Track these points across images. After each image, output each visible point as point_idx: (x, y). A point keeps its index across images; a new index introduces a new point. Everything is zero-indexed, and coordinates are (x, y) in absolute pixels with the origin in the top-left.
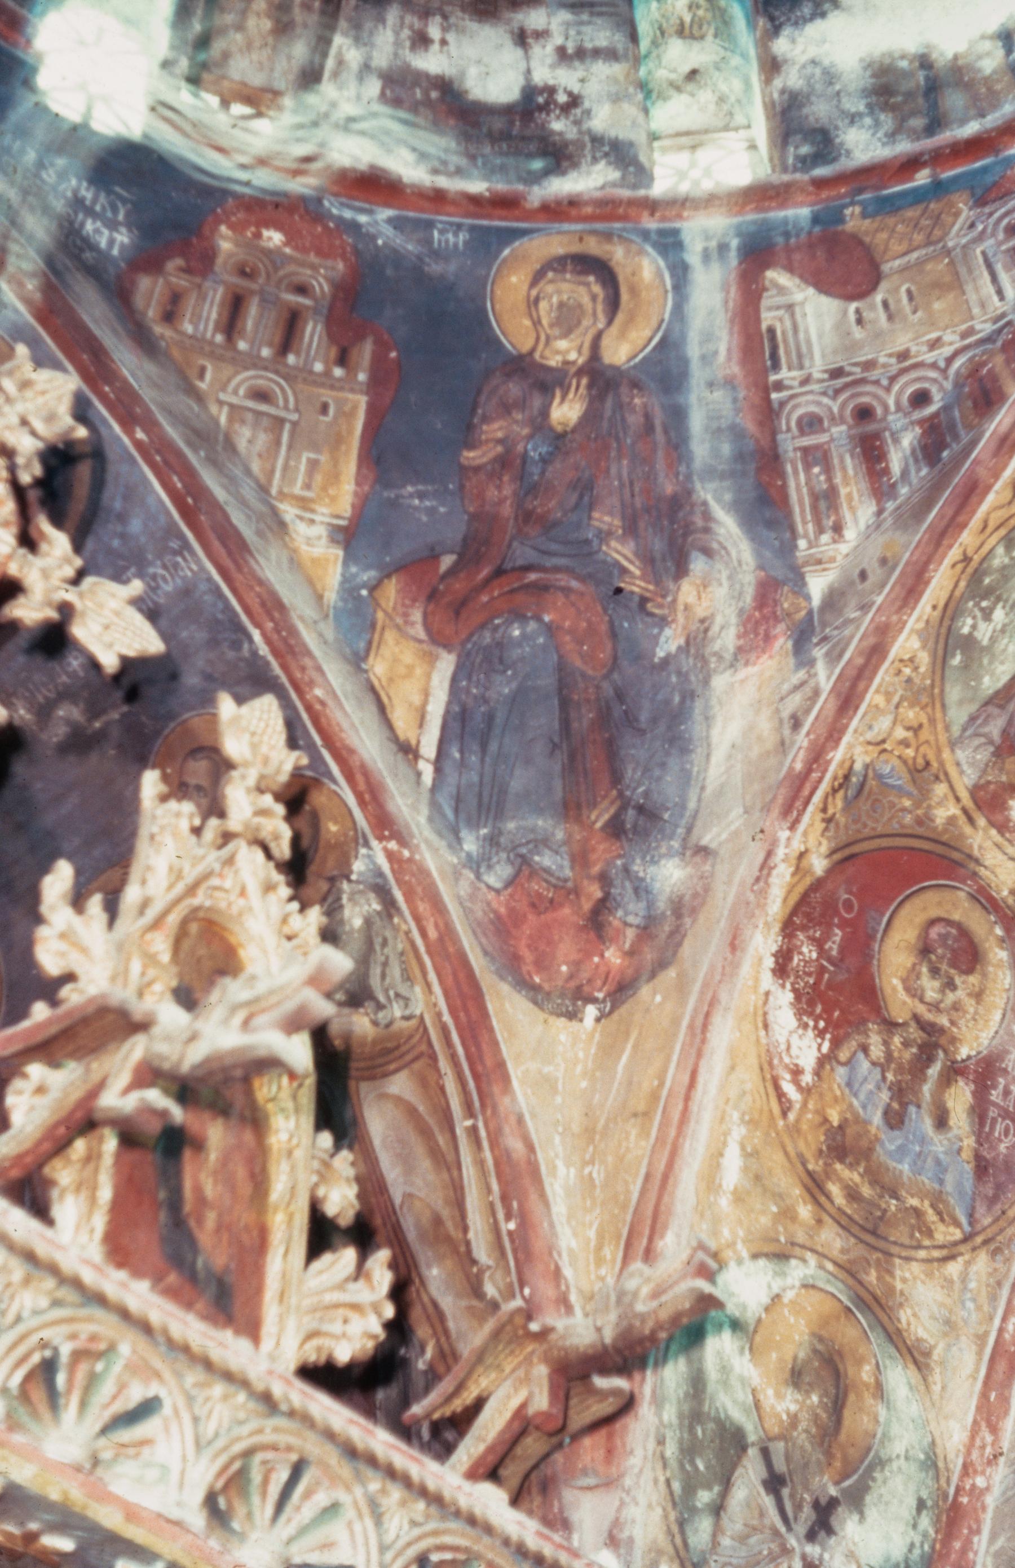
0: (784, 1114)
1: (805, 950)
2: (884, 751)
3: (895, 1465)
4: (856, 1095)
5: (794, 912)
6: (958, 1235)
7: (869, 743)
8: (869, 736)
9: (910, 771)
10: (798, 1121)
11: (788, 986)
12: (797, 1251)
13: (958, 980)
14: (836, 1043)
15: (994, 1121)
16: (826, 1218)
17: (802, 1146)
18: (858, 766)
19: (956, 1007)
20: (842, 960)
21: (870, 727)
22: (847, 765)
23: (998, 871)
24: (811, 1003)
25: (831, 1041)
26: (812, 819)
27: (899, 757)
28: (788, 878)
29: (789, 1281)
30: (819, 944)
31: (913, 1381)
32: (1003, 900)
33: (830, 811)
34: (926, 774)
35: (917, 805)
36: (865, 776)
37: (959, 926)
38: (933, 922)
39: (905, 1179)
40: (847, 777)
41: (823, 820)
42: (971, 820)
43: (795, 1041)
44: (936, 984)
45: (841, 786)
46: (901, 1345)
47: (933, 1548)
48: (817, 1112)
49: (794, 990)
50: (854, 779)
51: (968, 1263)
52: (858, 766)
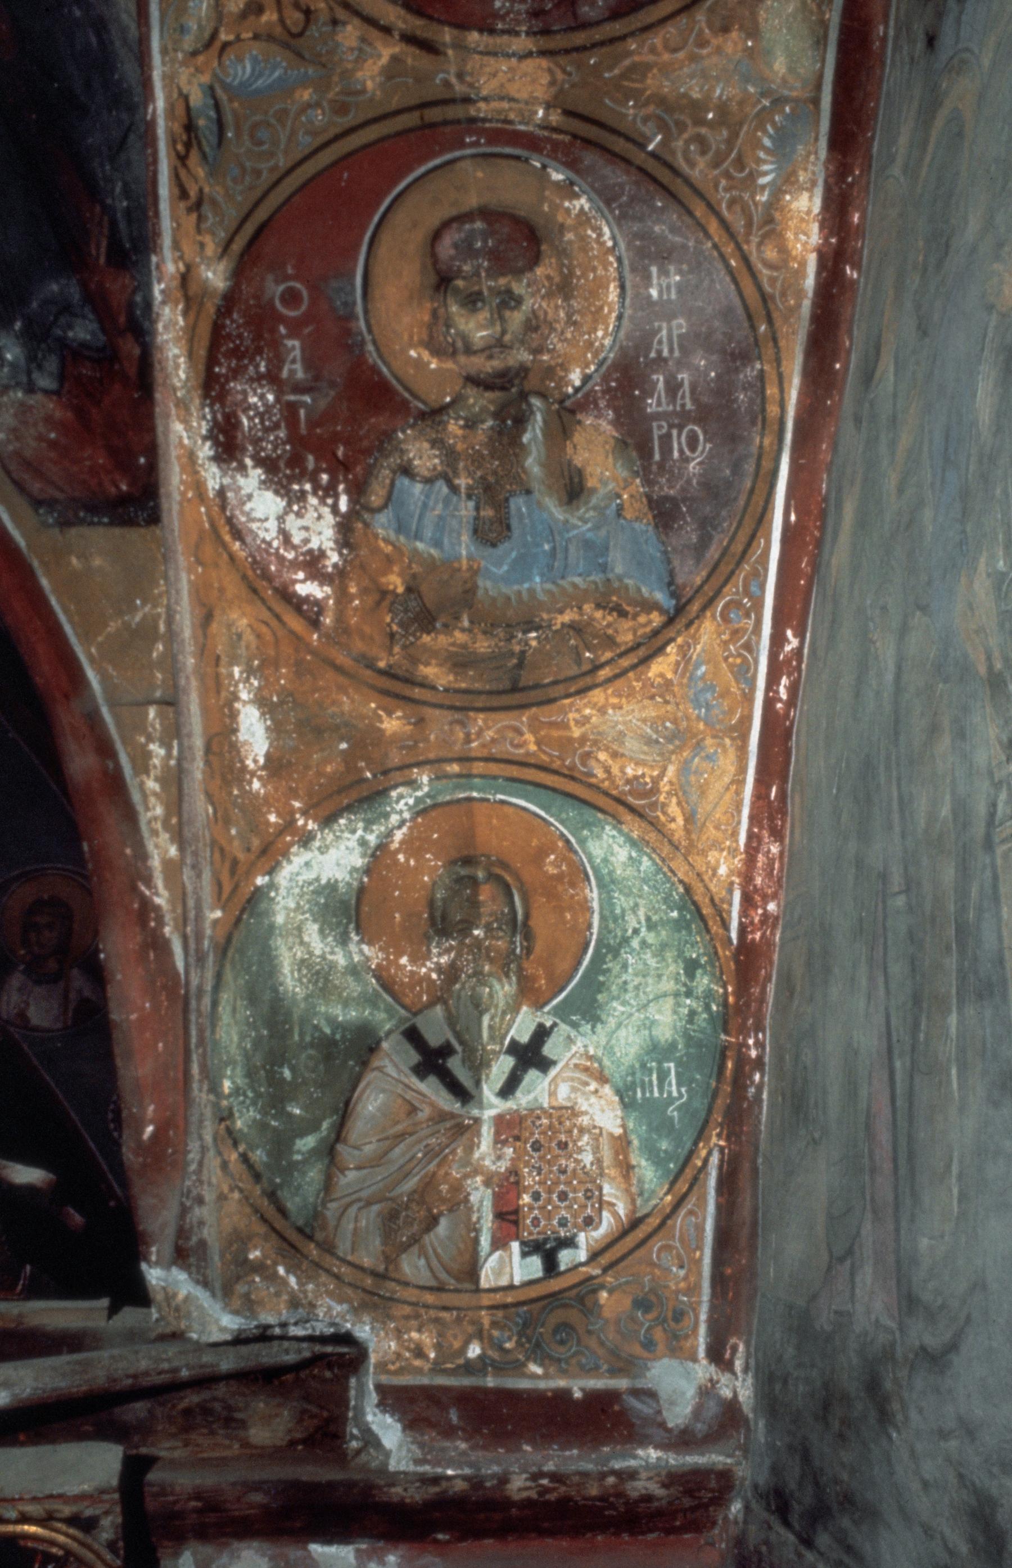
0: (315, 623)
1: (253, 400)
2: (226, 45)
3: (635, 943)
4: (418, 536)
5: (212, 360)
6: (656, 619)
7: (194, 54)
8: (189, 42)
9: (286, 46)
10: (340, 618)
11: (249, 462)
12: (397, 776)
13: (519, 288)
14: (358, 491)
15: (666, 440)
16: (429, 712)
17: (359, 645)
18: (197, 98)
19: (533, 325)
20: (317, 378)
21: (183, 30)
22: (180, 111)
23: (513, 90)
24: (295, 461)
25: (348, 491)
26: (174, 218)
27: (256, 37)
28: (181, 322)
29: (394, 819)
30: (272, 378)
31: (635, 835)
32: (545, 126)
33: (193, 193)
34: (313, 31)
35: (322, 85)
36: (217, 106)
37: (484, 213)
38: (436, 236)
39: (541, 596)
40: (190, 127)
41: (190, 210)
42: (429, 47)
43: (292, 523)
44: (484, 315)
45: (188, 145)
46: (602, 801)
47: (725, 1004)
48: (364, 591)
49: (259, 462)
50: (201, 122)
51: (684, 651)
52: (197, 98)
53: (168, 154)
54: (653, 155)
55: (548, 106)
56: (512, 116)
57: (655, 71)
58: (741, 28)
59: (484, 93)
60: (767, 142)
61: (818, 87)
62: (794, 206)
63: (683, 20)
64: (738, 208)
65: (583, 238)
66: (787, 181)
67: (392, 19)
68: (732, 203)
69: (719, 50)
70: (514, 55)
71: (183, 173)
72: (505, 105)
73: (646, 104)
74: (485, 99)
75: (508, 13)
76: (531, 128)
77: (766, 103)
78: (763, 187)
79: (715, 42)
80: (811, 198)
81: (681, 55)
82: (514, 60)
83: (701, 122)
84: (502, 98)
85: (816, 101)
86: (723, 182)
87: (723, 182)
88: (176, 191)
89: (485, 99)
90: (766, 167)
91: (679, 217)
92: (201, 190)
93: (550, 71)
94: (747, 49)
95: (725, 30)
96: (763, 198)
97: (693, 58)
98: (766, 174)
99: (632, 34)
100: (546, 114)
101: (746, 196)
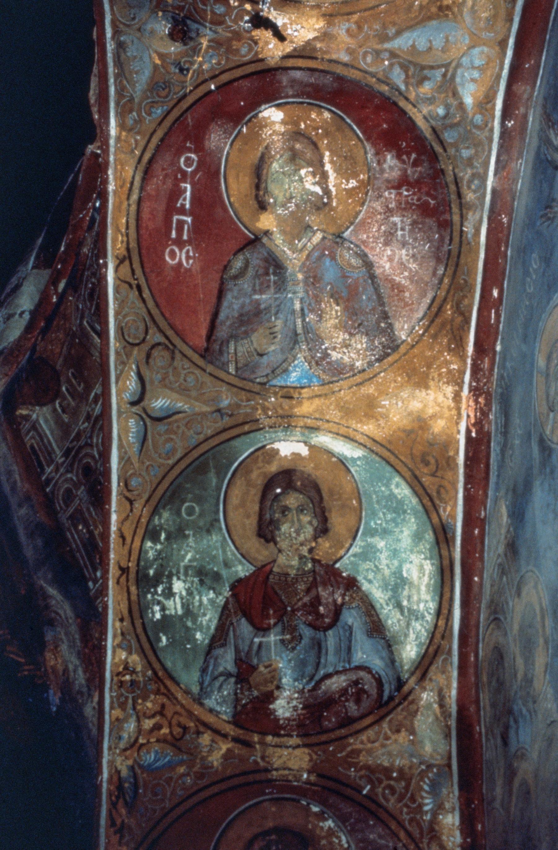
2: (142, 745)
7: (125, 750)
8: (122, 745)
9: (173, 745)
18: (124, 773)
21: (120, 738)
22: (115, 778)
23: (290, 764)
26: (107, 836)
27: (158, 741)
32: (308, 782)
33: (119, 822)
34: (187, 737)
35: (191, 764)
36: (135, 776)
37: (276, 830)
40: (120, 787)
41: (115, 833)
45: (118, 797)
50: (126, 785)
52: (124, 773)
53: (107, 802)
54: (365, 796)
55: (309, 772)
56: (290, 778)
57: (364, 753)
58: (407, 730)
59: (275, 766)
60: (426, 788)
61: (450, 758)
62: (445, 821)
63: (376, 728)
64: (414, 824)
65: (331, 843)
66: (439, 808)
67: (228, 730)
68: (411, 820)
69: (396, 741)
70: (290, 746)
71: (114, 811)
72: (287, 772)
73: (361, 769)
74: (277, 770)
75: (286, 727)
76: (300, 784)
77: (423, 767)
78: (427, 812)
79: (393, 737)
80: (453, 817)
81: (376, 744)
82: (290, 749)
83: (390, 778)
84: (285, 769)
85: (449, 766)
86: (405, 810)
87: (405, 810)
88: (109, 823)
89: (277, 770)
90: (427, 801)
91: (383, 830)
92: (123, 821)
93: (310, 754)
94: (410, 740)
95: (398, 731)
96: (428, 817)
97: (383, 746)
98: (427, 804)
99: (351, 735)
100: (308, 776)
101: (418, 817)
